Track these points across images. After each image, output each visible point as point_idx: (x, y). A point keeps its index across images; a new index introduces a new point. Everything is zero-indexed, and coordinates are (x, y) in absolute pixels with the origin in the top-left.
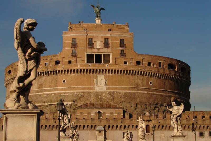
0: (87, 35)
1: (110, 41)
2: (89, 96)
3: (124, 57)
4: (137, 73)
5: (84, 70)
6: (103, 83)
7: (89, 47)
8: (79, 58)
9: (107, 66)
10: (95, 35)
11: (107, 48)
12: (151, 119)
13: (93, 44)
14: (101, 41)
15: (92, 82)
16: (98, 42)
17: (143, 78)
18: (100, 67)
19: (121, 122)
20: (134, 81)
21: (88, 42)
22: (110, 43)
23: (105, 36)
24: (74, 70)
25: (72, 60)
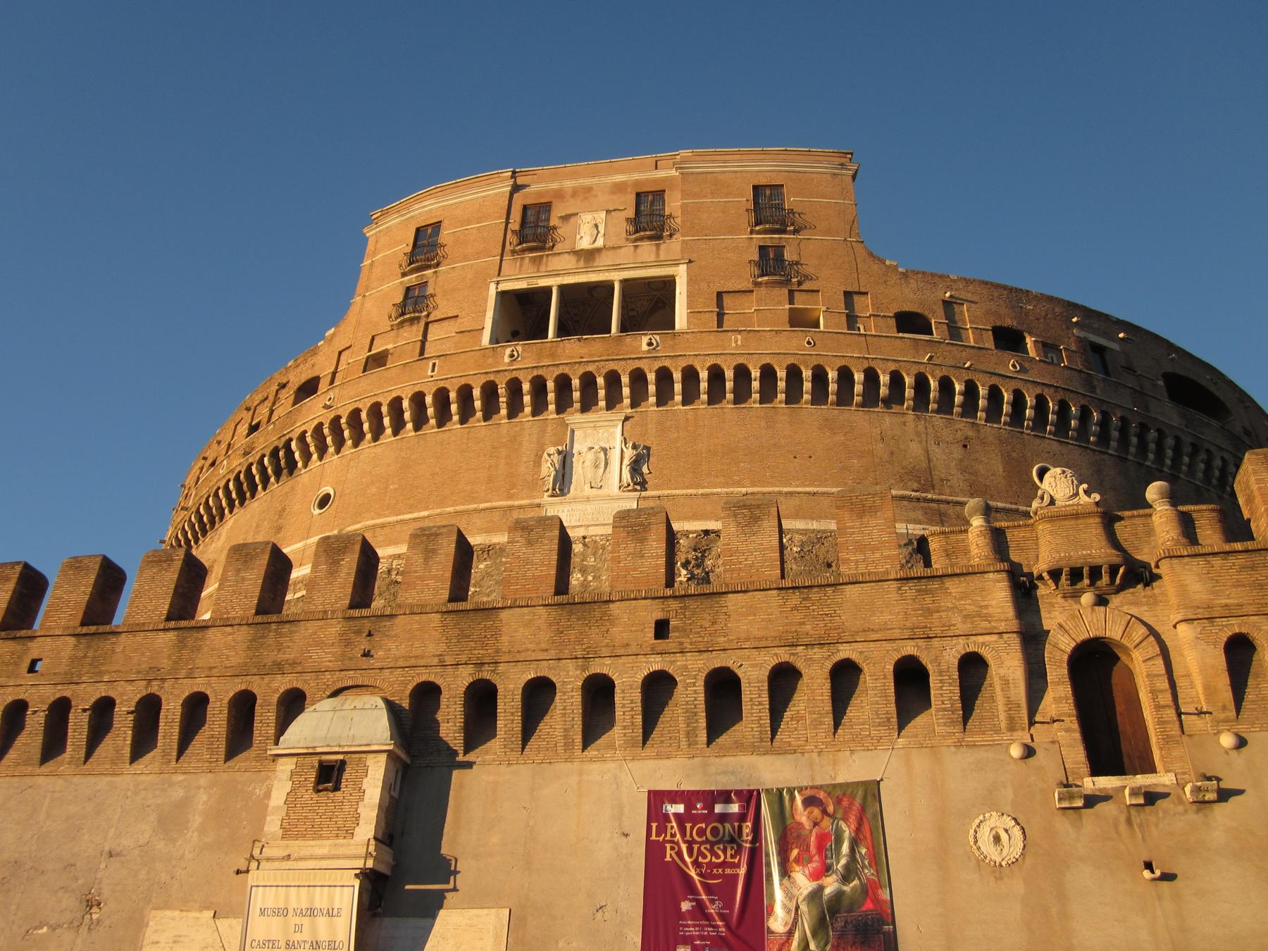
0: (516, 188)
1: (673, 205)
2: (489, 575)
3: (788, 282)
4: (909, 393)
5: (465, 393)
6: (618, 472)
7: (523, 251)
8: (446, 323)
9: (645, 347)
10: (569, 184)
11: (650, 238)
12: (1144, 555)
13: (555, 228)
14: (608, 212)
15: (522, 469)
16: (586, 220)
17: (971, 433)
18: (590, 355)
19: (662, 629)
20: (892, 453)
21: (515, 224)
22: (677, 213)
23: (637, 183)
24: (396, 404)
25: (390, 346)
